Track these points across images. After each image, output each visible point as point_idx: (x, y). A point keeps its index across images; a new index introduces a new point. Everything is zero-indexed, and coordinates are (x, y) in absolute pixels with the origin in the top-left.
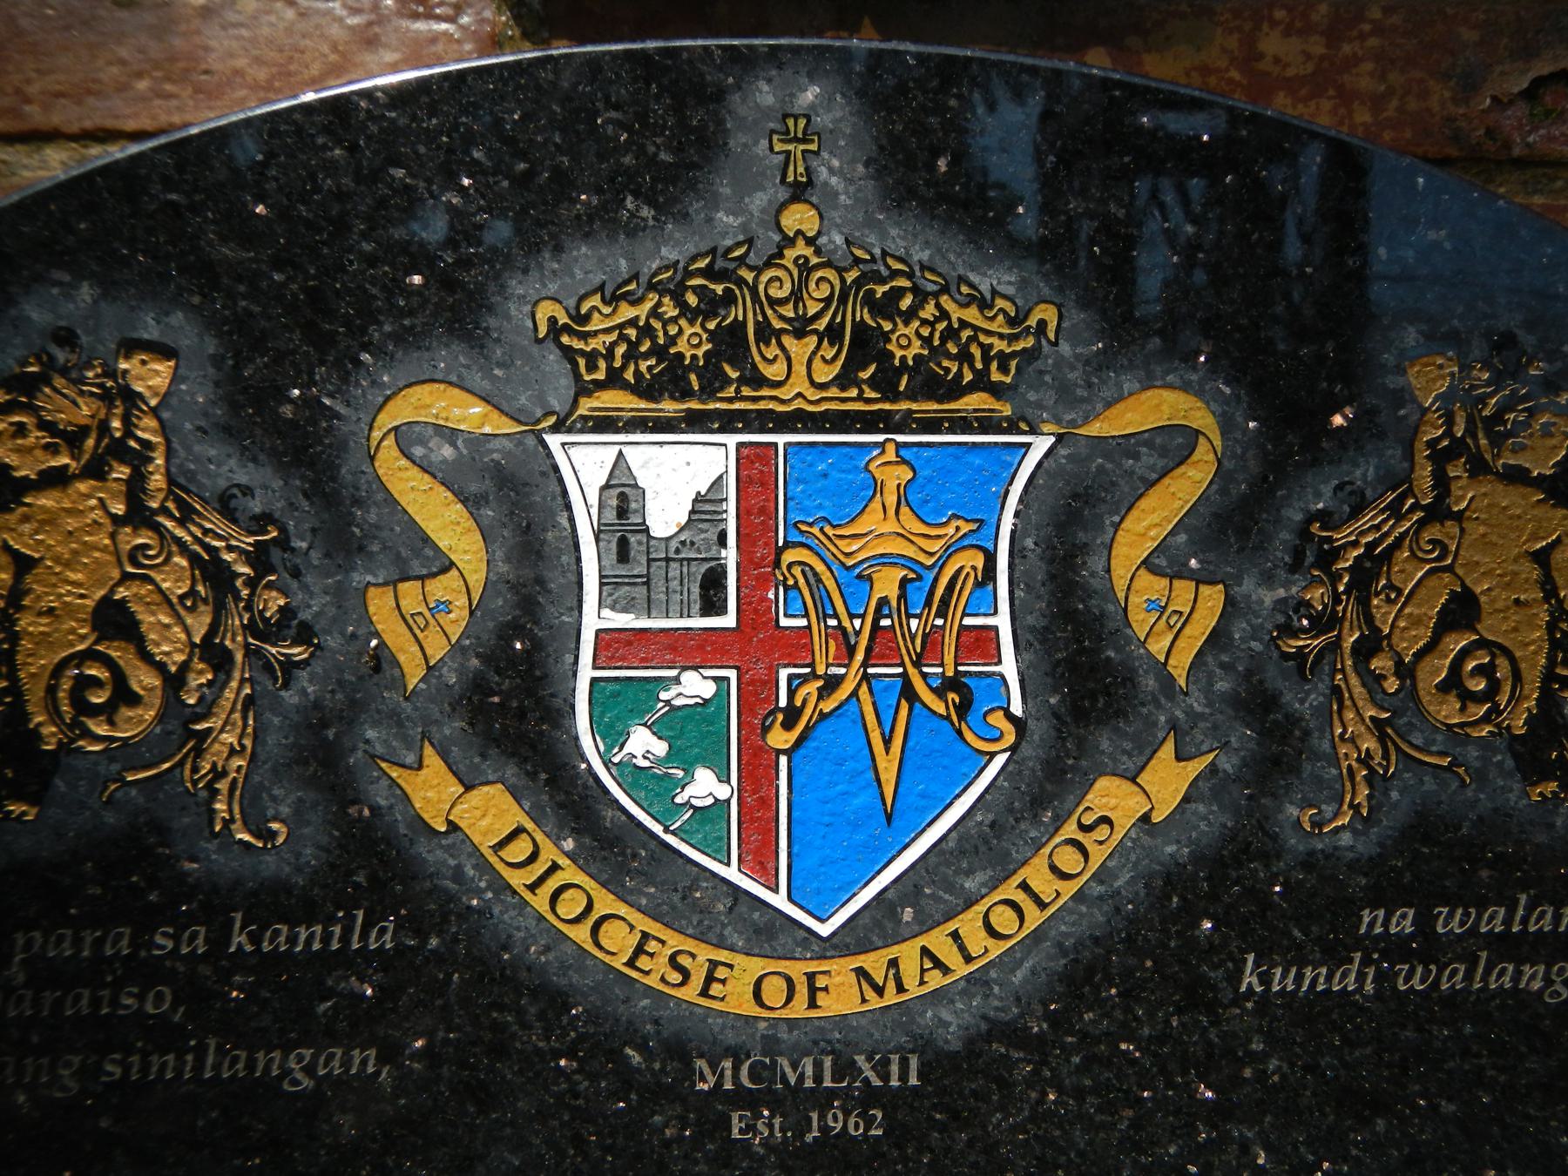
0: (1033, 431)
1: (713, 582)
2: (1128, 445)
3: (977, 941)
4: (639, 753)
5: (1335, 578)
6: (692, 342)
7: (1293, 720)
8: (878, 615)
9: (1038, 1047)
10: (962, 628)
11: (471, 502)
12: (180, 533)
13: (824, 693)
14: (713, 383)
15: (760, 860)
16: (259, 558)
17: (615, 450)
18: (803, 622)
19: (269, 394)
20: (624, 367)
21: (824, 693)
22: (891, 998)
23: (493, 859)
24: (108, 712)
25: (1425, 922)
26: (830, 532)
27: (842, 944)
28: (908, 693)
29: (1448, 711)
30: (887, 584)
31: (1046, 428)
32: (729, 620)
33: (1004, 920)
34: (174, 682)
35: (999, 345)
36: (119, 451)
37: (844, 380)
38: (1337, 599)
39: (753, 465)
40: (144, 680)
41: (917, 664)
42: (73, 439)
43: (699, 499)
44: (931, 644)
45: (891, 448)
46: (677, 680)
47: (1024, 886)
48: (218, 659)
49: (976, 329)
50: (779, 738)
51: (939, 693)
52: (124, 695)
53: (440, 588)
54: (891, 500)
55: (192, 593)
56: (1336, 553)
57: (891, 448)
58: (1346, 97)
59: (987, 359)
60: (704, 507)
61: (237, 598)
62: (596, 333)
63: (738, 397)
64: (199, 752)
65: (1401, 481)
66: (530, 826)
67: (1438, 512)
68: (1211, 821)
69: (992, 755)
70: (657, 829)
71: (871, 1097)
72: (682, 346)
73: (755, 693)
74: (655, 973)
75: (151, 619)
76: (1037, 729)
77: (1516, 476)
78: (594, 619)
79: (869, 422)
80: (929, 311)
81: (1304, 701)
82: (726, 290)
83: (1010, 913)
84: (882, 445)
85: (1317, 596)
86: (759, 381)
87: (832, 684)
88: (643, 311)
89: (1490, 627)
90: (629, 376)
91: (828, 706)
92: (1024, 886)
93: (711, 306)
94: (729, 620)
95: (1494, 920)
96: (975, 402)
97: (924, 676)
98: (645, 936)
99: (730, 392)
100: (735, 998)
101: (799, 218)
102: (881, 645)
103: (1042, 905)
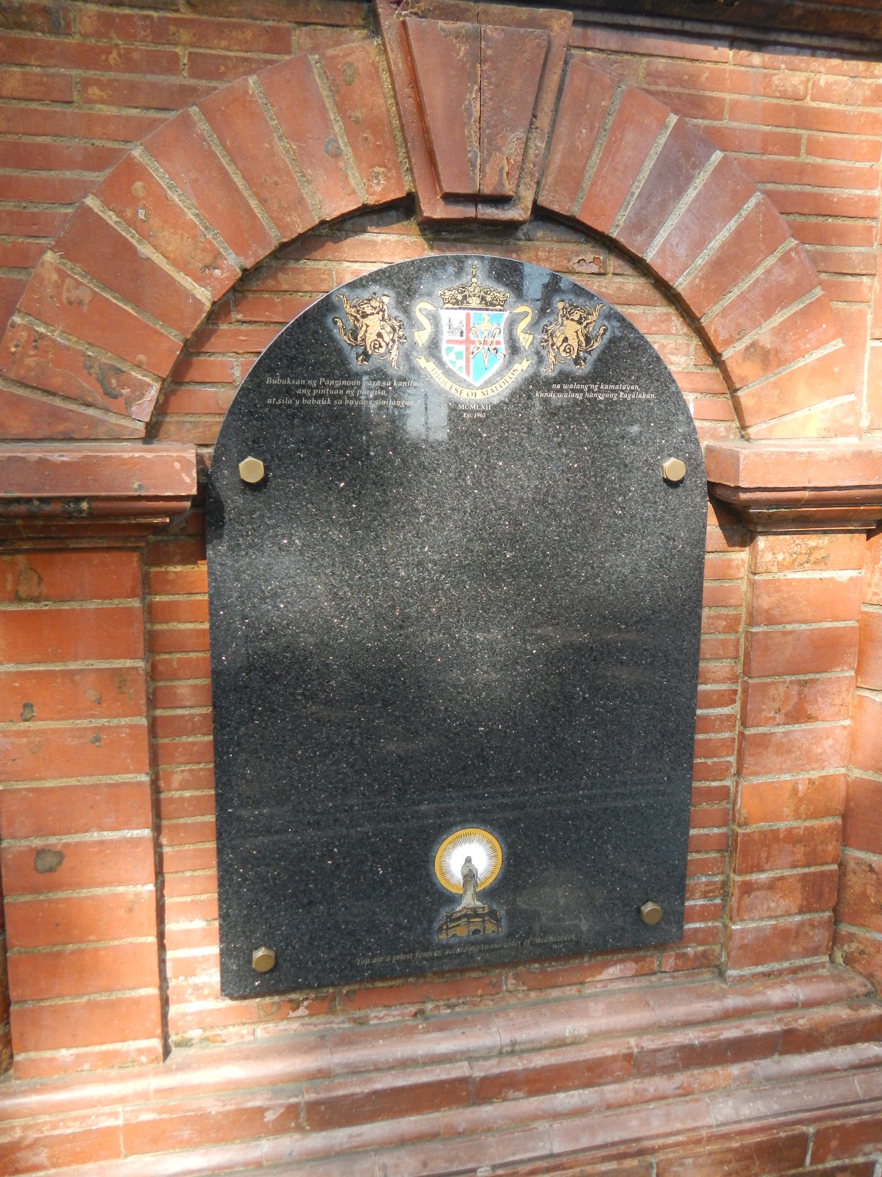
1: (462, 332)
2: (519, 314)
6: (460, 297)
7: (542, 356)
9: (507, 404)
11: (429, 319)
14: (462, 303)
16: (400, 327)
19: (401, 303)
24: (378, 349)
25: (562, 387)
27: (480, 388)
29: (564, 354)
30: (486, 334)
33: (502, 385)
34: (387, 344)
36: (381, 310)
37: (481, 303)
40: (383, 344)
42: (375, 308)
44: (492, 342)
48: (393, 341)
50: (471, 356)
52: (380, 346)
58: (551, 262)
65: (556, 320)
67: (562, 325)
68: (531, 371)
71: (484, 411)
73: (467, 349)
74: (453, 391)
75: (385, 335)
76: (507, 356)
77: (572, 320)
78: (445, 336)
81: (544, 352)
85: (546, 337)
86: (468, 303)
89: (569, 342)
94: (464, 338)
95: (571, 386)
100: (464, 395)
101: (474, 280)
102: (485, 342)
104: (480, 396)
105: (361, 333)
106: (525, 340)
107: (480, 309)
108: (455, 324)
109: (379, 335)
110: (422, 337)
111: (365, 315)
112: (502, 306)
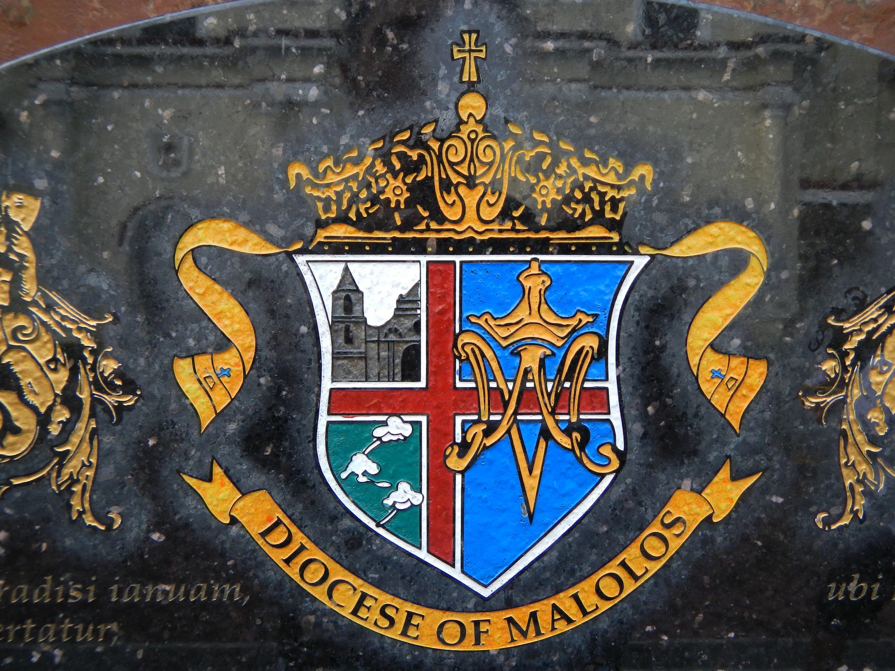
0: (636, 253)
3: (590, 600)
4: (359, 472)
5: (844, 354)
8: (525, 379)
10: (583, 389)
12: (45, 318)
13: (487, 433)
17: (342, 265)
18: (473, 385)
20: (349, 208)
21: (487, 433)
22: (532, 639)
23: (260, 541)
26: (492, 323)
28: (545, 434)
31: (642, 250)
32: (422, 384)
34: (44, 420)
35: (611, 193)
38: (845, 369)
40: (24, 419)
41: (553, 413)
43: (401, 300)
45: (535, 265)
46: (385, 424)
47: (623, 564)
49: (595, 181)
51: (568, 432)
54: (535, 301)
55: (54, 360)
56: (846, 338)
57: (535, 265)
59: (602, 203)
61: (85, 363)
62: (328, 186)
63: (428, 229)
64: (61, 466)
66: (286, 521)
69: (603, 476)
70: (372, 525)
72: (389, 194)
74: (370, 619)
79: (521, 246)
80: (562, 170)
82: (421, 156)
83: (614, 584)
84: (529, 262)
86: (442, 219)
87: (491, 428)
88: (360, 170)
90: (352, 216)
91: (489, 442)
92: (623, 564)
93: (411, 167)
96: (596, 232)
97: (557, 422)
98: (364, 596)
99: (422, 226)
102: (526, 398)
103: (636, 578)
107: (500, 246)
112: (612, 226)
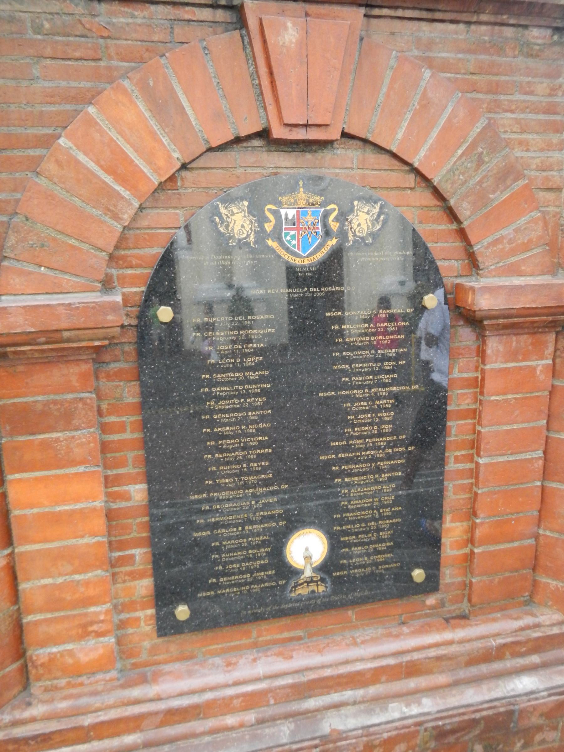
14: (294, 204)
15: (299, 249)
30: (310, 223)
39: (298, 212)
52: (243, 233)
53: (271, 224)
60: (294, 216)
67: (357, 215)
73: (298, 233)
74: (290, 260)
78: (284, 227)
100: (297, 262)
104: (306, 262)
105: (231, 225)
106: (334, 226)
108: (290, 217)
109: (243, 226)
110: (269, 227)
111: (233, 214)
